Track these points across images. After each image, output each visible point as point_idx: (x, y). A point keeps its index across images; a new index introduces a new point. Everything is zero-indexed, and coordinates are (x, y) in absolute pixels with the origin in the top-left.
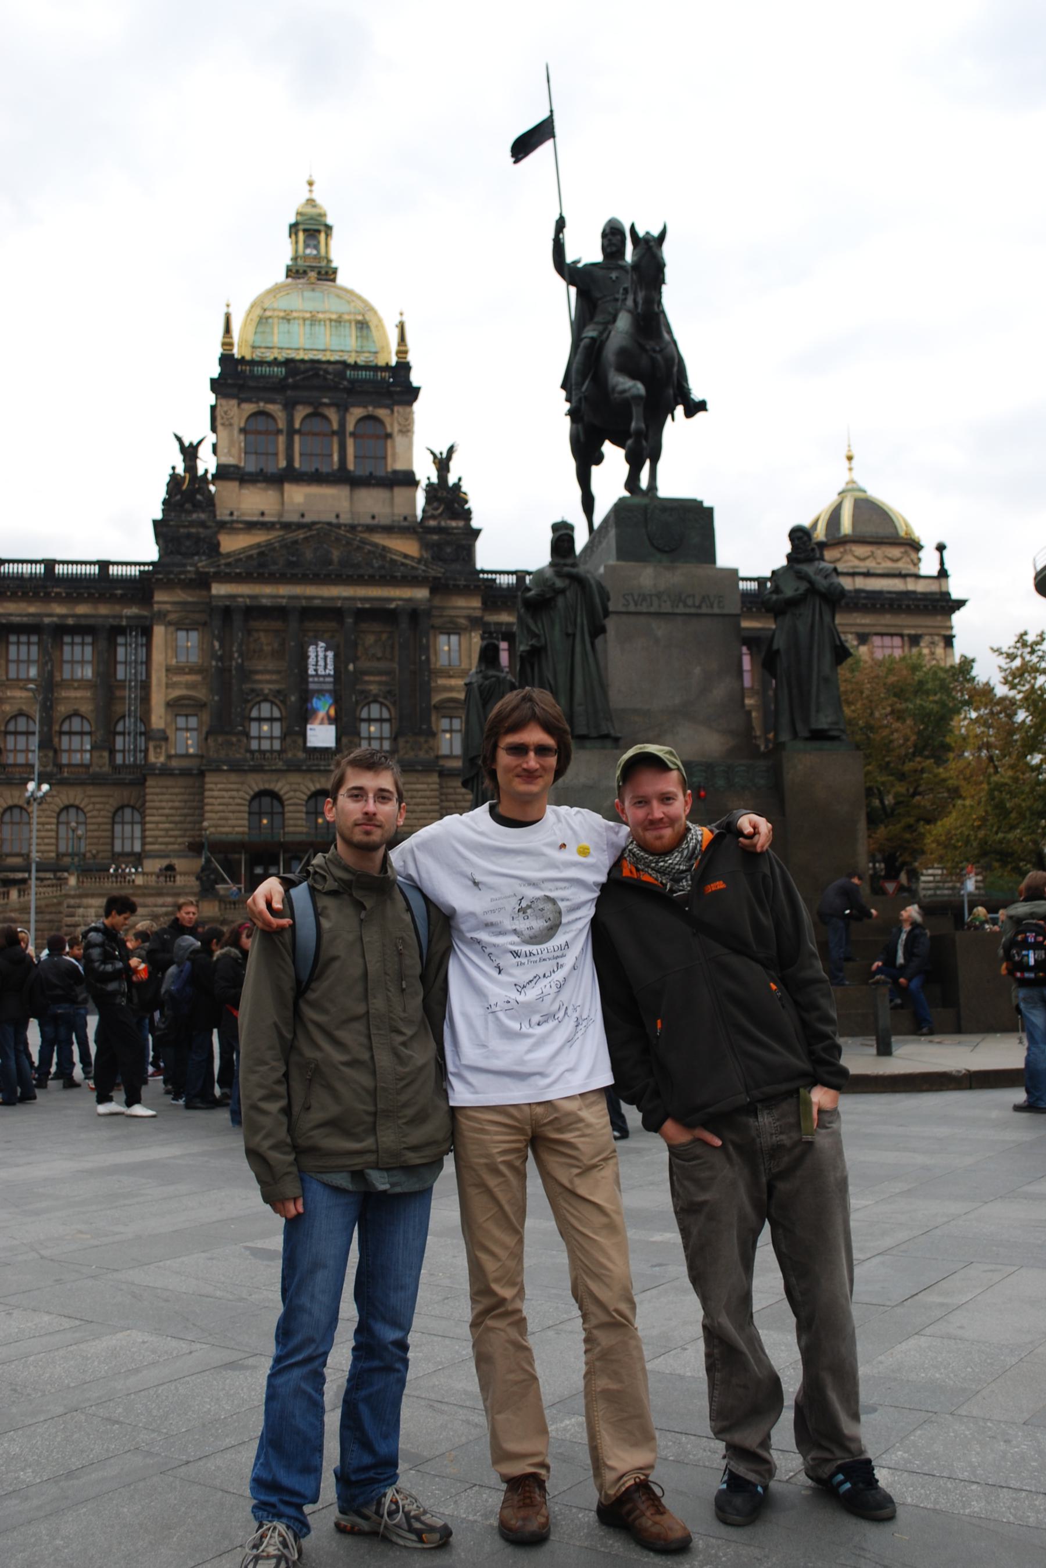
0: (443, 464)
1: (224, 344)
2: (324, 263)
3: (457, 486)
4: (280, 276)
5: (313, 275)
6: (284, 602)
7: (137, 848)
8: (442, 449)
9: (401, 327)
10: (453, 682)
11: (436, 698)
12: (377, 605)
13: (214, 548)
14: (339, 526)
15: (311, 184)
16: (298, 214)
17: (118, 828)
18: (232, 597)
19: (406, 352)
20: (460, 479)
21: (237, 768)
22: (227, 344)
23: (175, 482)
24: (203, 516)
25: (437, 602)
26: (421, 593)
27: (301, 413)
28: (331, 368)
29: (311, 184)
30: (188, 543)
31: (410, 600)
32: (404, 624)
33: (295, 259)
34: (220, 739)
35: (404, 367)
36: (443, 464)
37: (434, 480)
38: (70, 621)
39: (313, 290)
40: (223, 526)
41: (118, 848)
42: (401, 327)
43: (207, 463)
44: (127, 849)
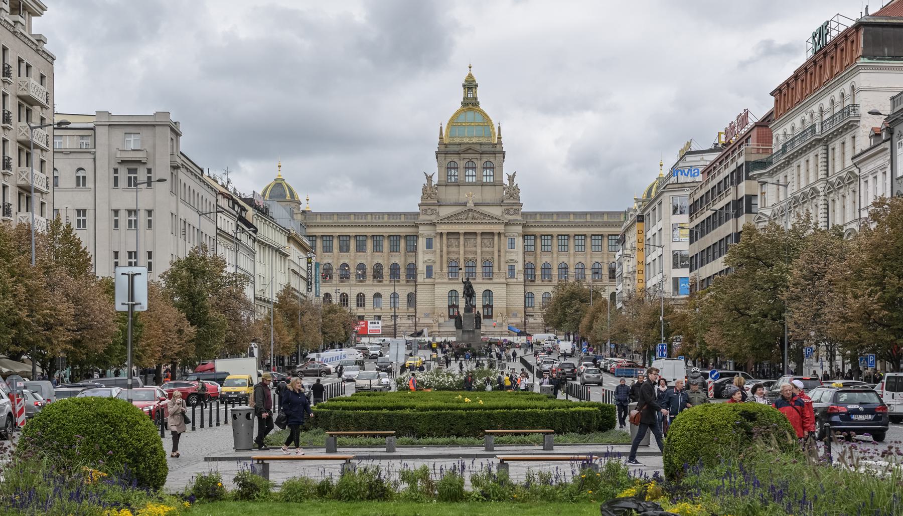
0: (511, 179)
1: (440, 138)
2: (474, 101)
4: (459, 106)
8: (511, 174)
9: (499, 127)
15: (470, 67)
16: (466, 81)
19: (501, 138)
20: (517, 185)
22: (441, 138)
23: (425, 189)
29: (470, 67)
30: (429, 211)
32: (496, 238)
33: (464, 98)
37: (508, 185)
42: (499, 127)
43: (435, 180)
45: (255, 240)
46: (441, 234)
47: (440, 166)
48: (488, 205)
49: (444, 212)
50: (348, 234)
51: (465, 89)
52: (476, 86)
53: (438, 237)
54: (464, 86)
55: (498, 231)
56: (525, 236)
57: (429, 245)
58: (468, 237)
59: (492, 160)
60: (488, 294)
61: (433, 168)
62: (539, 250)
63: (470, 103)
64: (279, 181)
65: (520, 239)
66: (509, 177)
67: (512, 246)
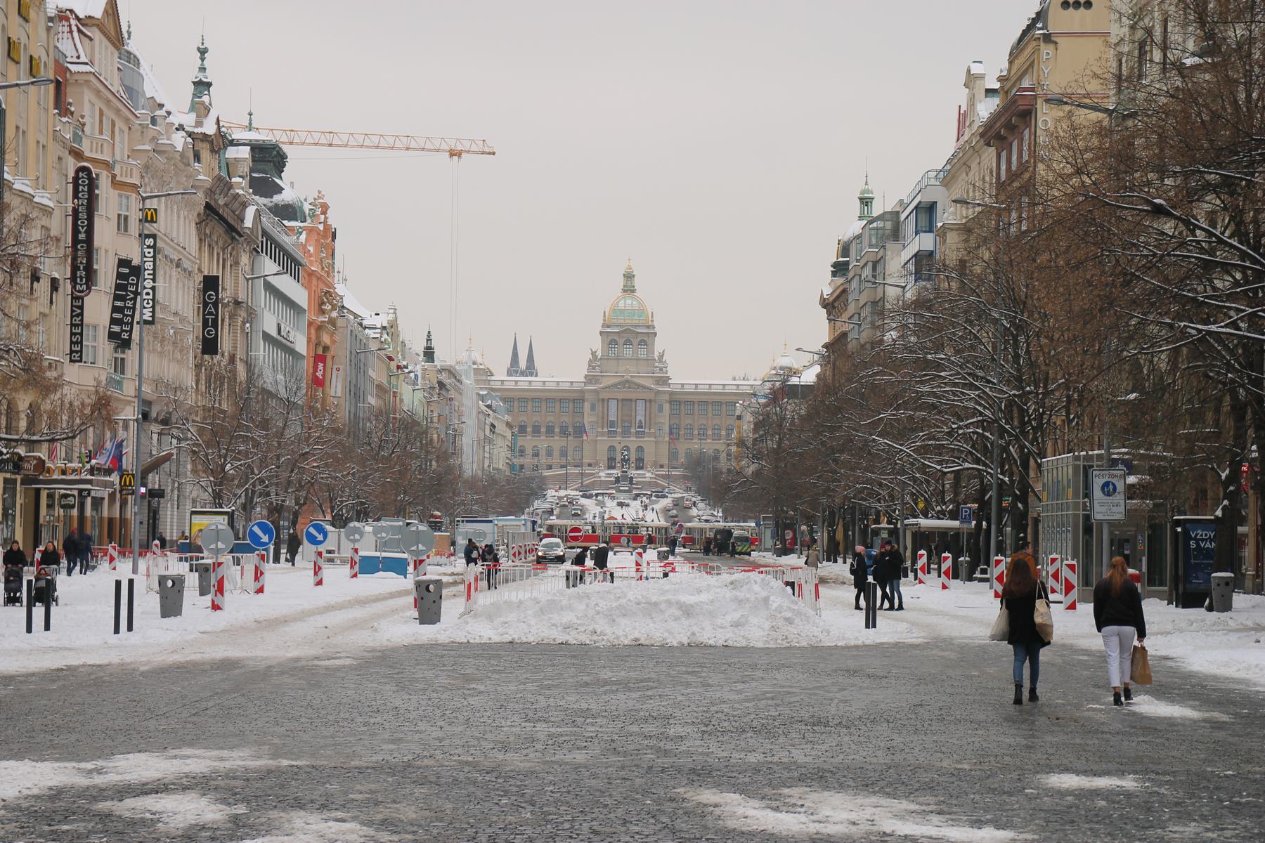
0: (661, 356)
33: (624, 286)
43: (599, 354)
45: (494, 433)
46: (603, 399)
47: (603, 341)
52: (634, 276)
53: (600, 402)
54: (624, 275)
56: (670, 402)
57: (593, 408)
58: (624, 402)
60: (640, 449)
61: (597, 344)
62: (683, 414)
63: (629, 290)
65: (668, 404)
67: (661, 409)
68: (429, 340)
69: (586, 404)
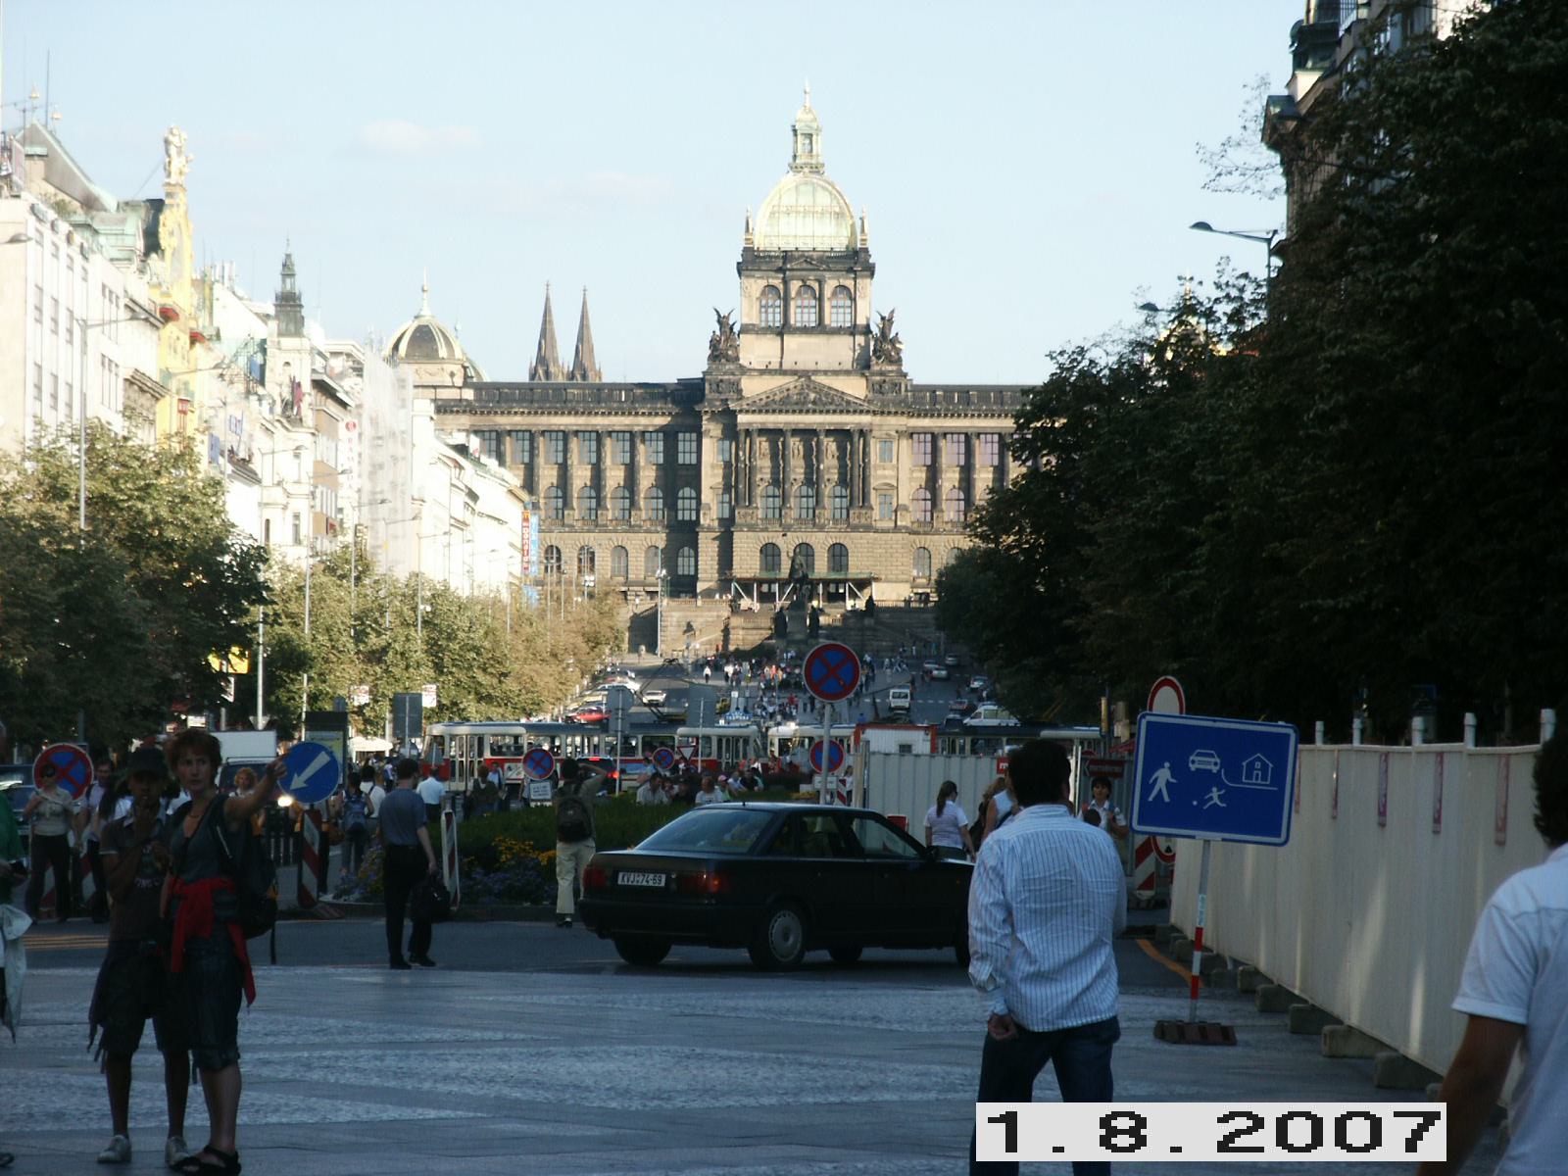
0: (887, 322)
3: (894, 341)
5: (806, 170)
6: (781, 426)
7: (692, 573)
9: (862, 219)
10: (887, 472)
11: (874, 483)
12: (838, 427)
13: (739, 391)
14: (816, 372)
17: (680, 559)
18: (751, 424)
21: (752, 528)
23: (714, 344)
24: (732, 367)
25: (877, 419)
26: (865, 419)
27: (795, 285)
28: (815, 254)
31: (859, 424)
33: (795, 157)
34: (743, 511)
35: (866, 250)
36: (887, 322)
38: (651, 429)
39: (806, 183)
40: (744, 371)
41: (680, 573)
42: (862, 219)
44: (686, 573)
46: (748, 433)
48: (836, 373)
49: (752, 387)
50: (562, 428)
51: (796, 135)
55: (859, 427)
59: (850, 283)
64: (423, 322)
66: (883, 318)
68: (288, 270)
69: (706, 441)
